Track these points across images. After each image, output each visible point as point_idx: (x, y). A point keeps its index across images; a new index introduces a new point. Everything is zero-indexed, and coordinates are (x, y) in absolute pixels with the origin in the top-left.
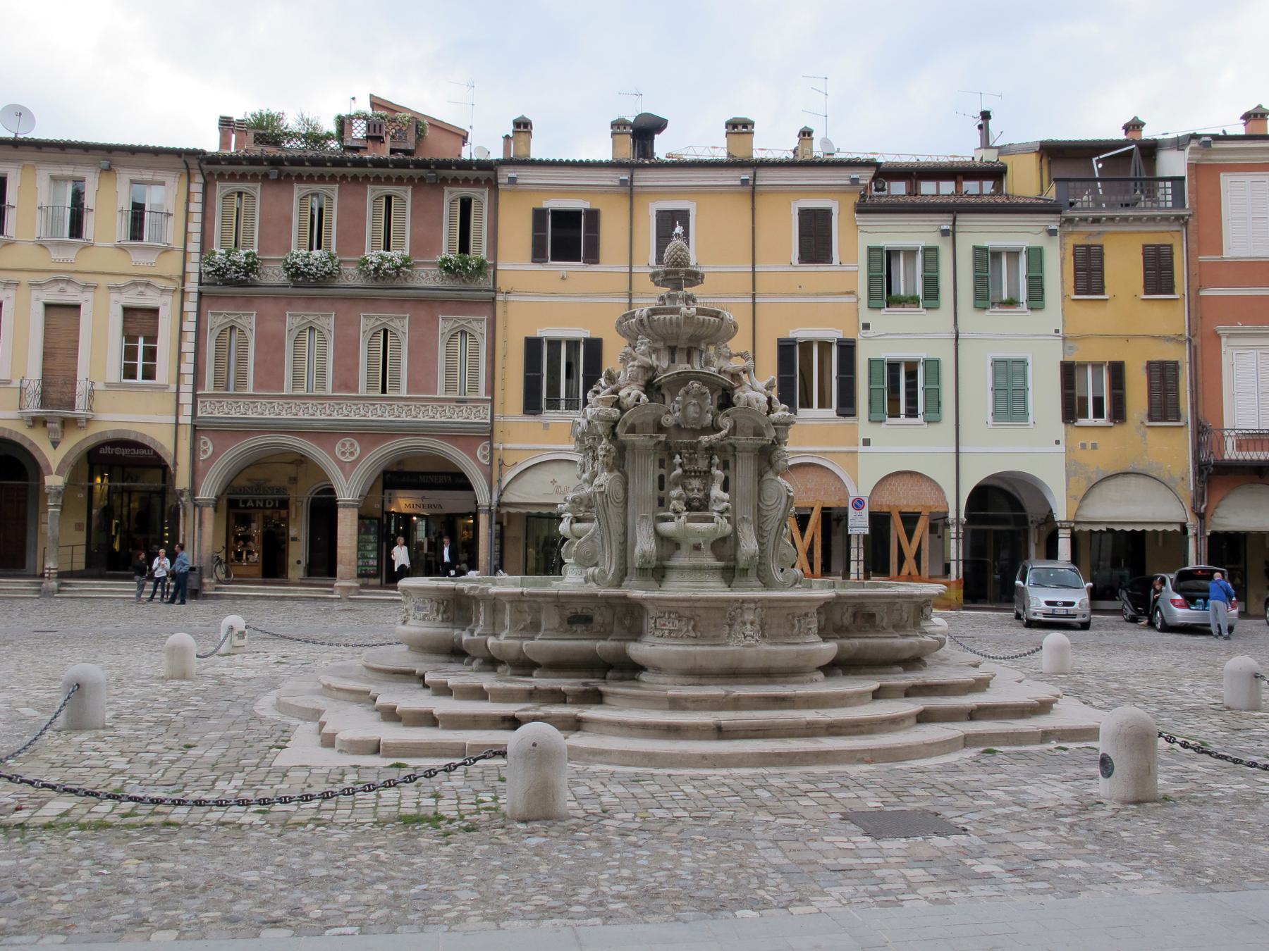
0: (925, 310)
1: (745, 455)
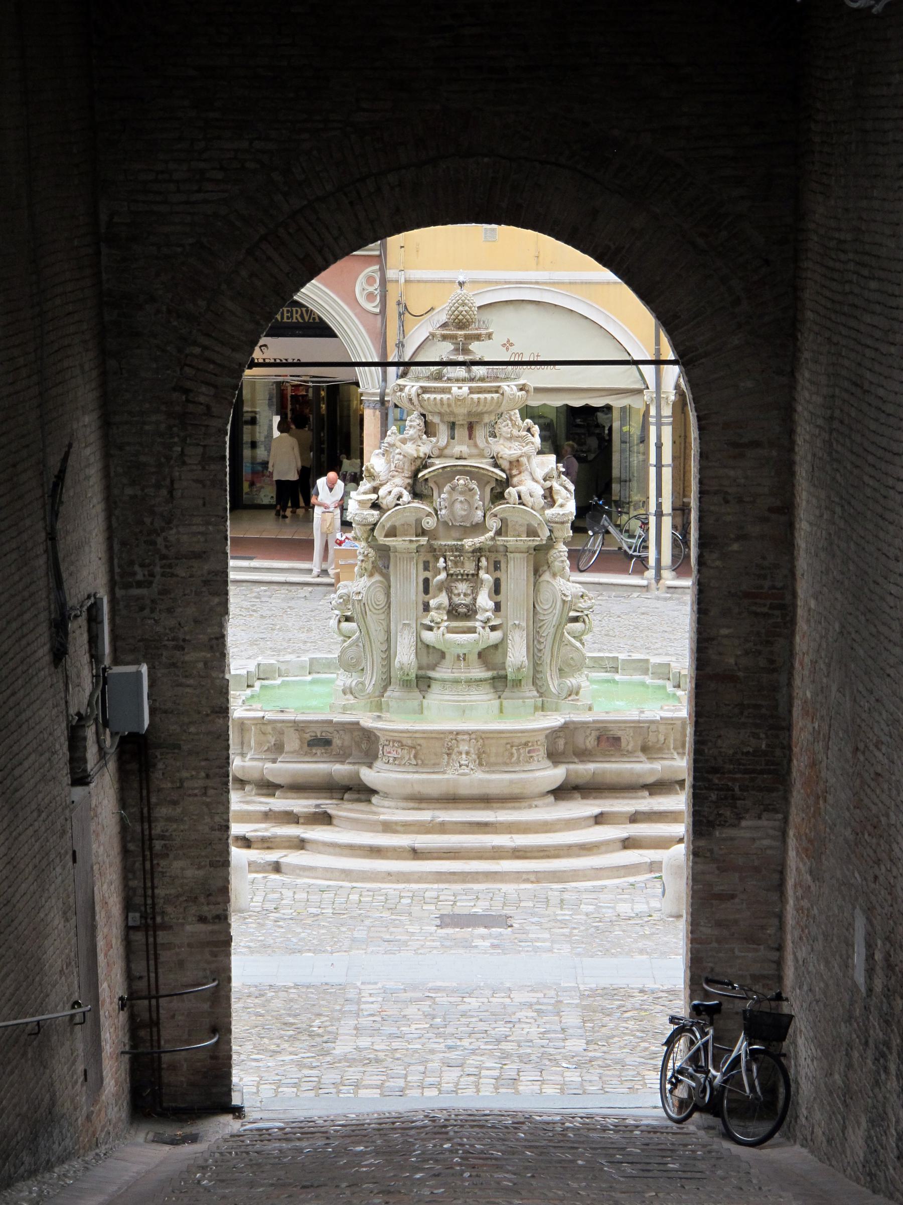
1: (517, 555)
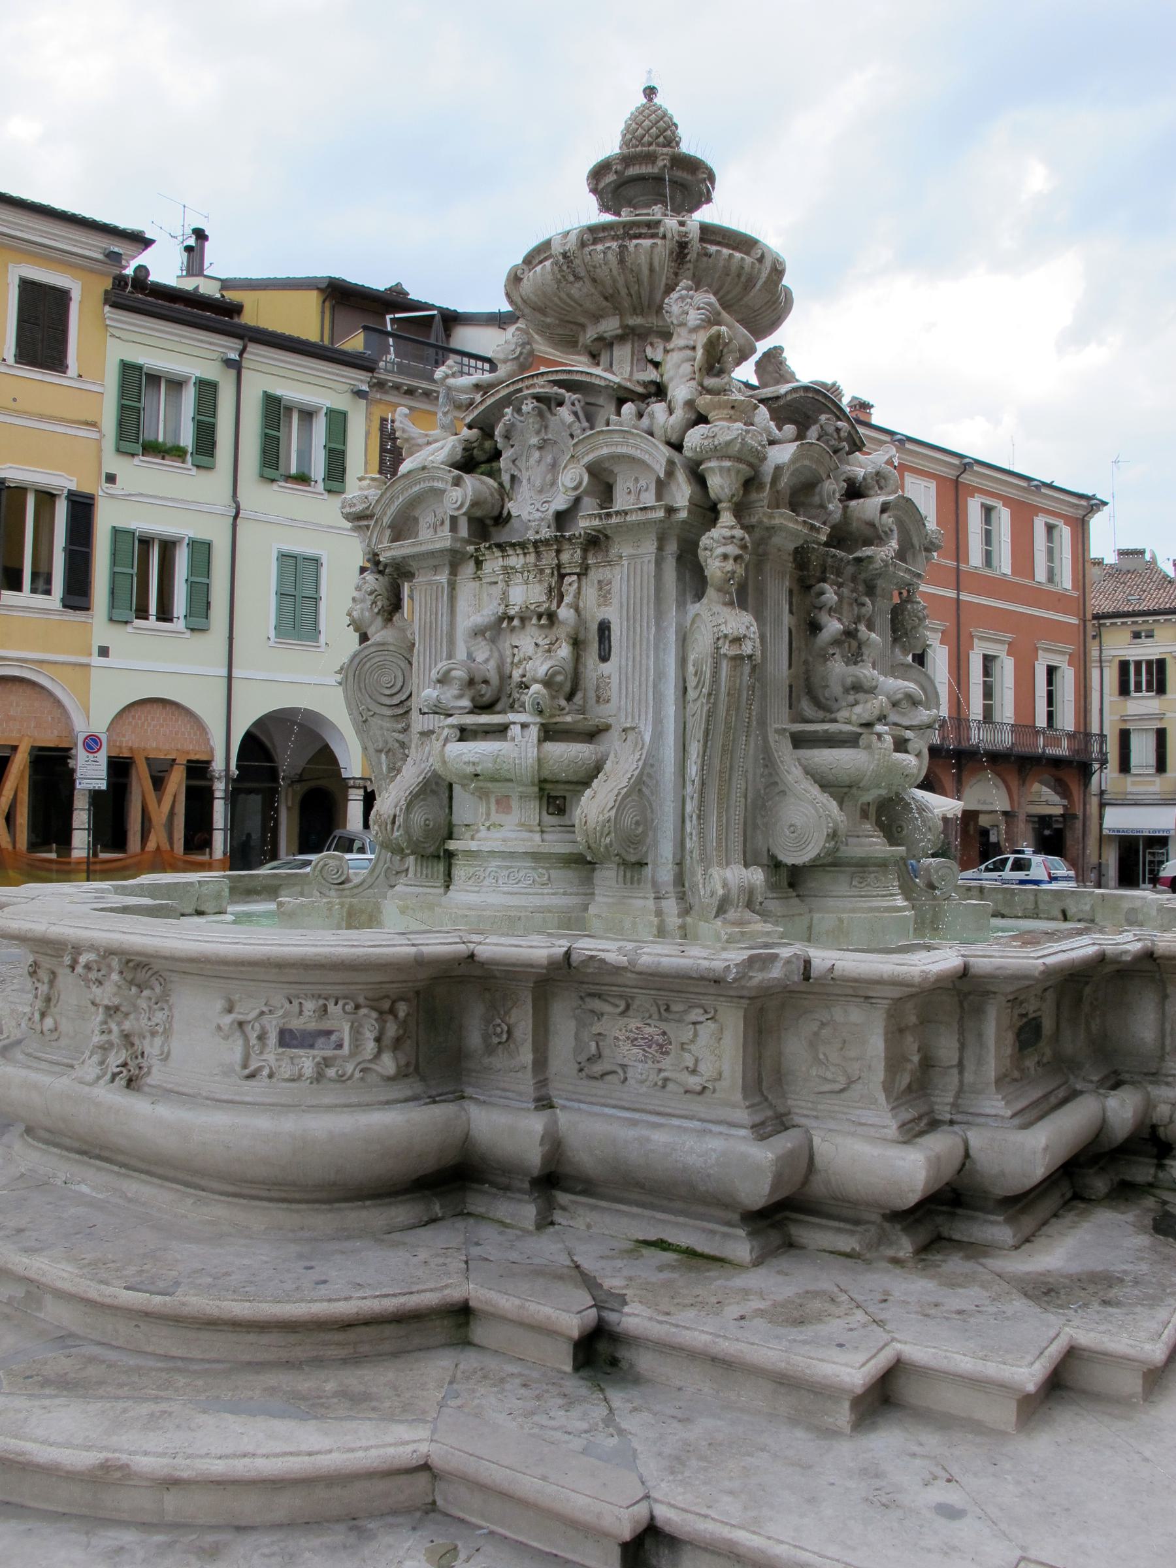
0: (195, 469)
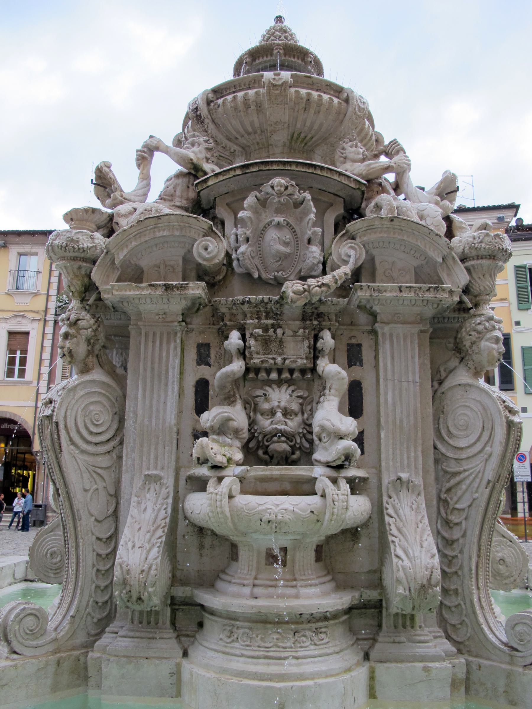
1: (400, 329)
